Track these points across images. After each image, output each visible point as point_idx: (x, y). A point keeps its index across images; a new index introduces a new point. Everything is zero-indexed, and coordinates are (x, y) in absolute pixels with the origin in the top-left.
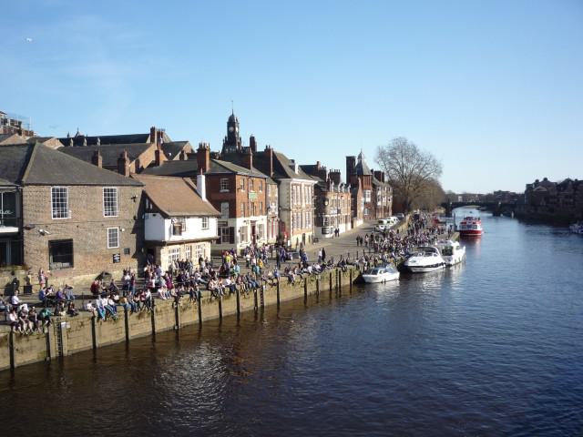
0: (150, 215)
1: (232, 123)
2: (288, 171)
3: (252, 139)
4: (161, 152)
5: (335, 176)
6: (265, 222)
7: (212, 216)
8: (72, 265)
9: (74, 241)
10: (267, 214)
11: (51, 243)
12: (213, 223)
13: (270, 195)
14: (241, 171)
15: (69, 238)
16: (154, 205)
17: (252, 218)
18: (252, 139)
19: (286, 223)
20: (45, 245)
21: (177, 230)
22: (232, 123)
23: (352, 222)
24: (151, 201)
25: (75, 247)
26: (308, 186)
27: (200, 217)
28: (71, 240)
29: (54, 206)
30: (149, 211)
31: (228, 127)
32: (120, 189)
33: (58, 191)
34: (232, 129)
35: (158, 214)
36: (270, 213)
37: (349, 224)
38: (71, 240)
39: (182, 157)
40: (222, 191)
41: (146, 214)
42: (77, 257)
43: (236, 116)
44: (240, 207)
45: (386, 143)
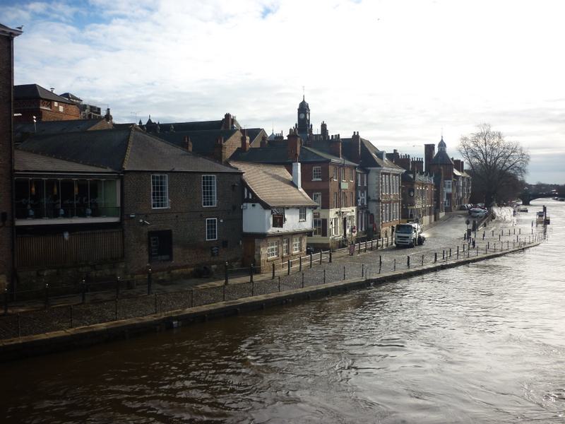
0: (250, 205)
1: (303, 109)
2: (377, 160)
3: (324, 126)
4: (248, 138)
5: (419, 163)
6: (354, 214)
7: (310, 207)
8: (171, 259)
9: (174, 233)
10: (356, 204)
11: (151, 234)
12: (309, 215)
13: (359, 185)
14: (335, 160)
15: (168, 229)
16: (254, 195)
17: (343, 209)
18: (324, 126)
19: (375, 215)
21: (279, 221)
22: (303, 109)
23: (435, 214)
24: (250, 191)
25: (174, 238)
26: (396, 175)
27: (298, 207)
28: (170, 232)
29: (154, 195)
30: (248, 201)
31: (299, 113)
32: (217, 177)
33: (157, 177)
34: (302, 116)
35: (258, 205)
36: (360, 205)
37: (433, 216)
38: (170, 232)
39: (262, 143)
40: (314, 180)
41: (245, 204)
42: (176, 250)
43: (306, 101)
44: (332, 198)
45: (470, 130)
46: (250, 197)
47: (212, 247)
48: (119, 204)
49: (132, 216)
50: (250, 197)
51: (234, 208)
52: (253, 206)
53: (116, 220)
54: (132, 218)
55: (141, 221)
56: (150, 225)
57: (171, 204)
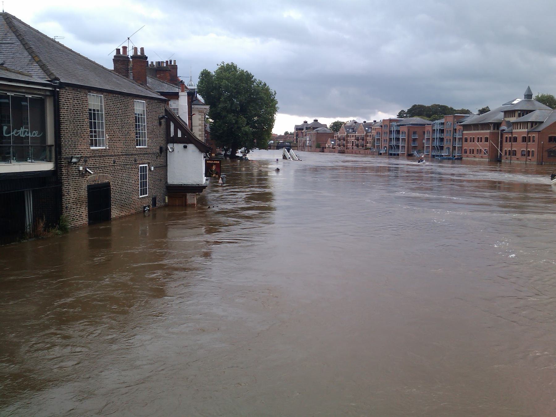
0: (178, 147)
15: (107, 181)
16: (184, 131)
20: (84, 193)
28: (108, 185)
30: (175, 140)
35: (191, 147)
38: (108, 185)
41: (170, 146)
46: (180, 135)
47: (145, 207)
48: (50, 140)
49: (74, 160)
50: (180, 135)
51: (161, 149)
52: (185, 147)
53: (48, 166)
54: (75, 163)
55: (81, 168)
56: (94, 177)
57: (110, 140)
